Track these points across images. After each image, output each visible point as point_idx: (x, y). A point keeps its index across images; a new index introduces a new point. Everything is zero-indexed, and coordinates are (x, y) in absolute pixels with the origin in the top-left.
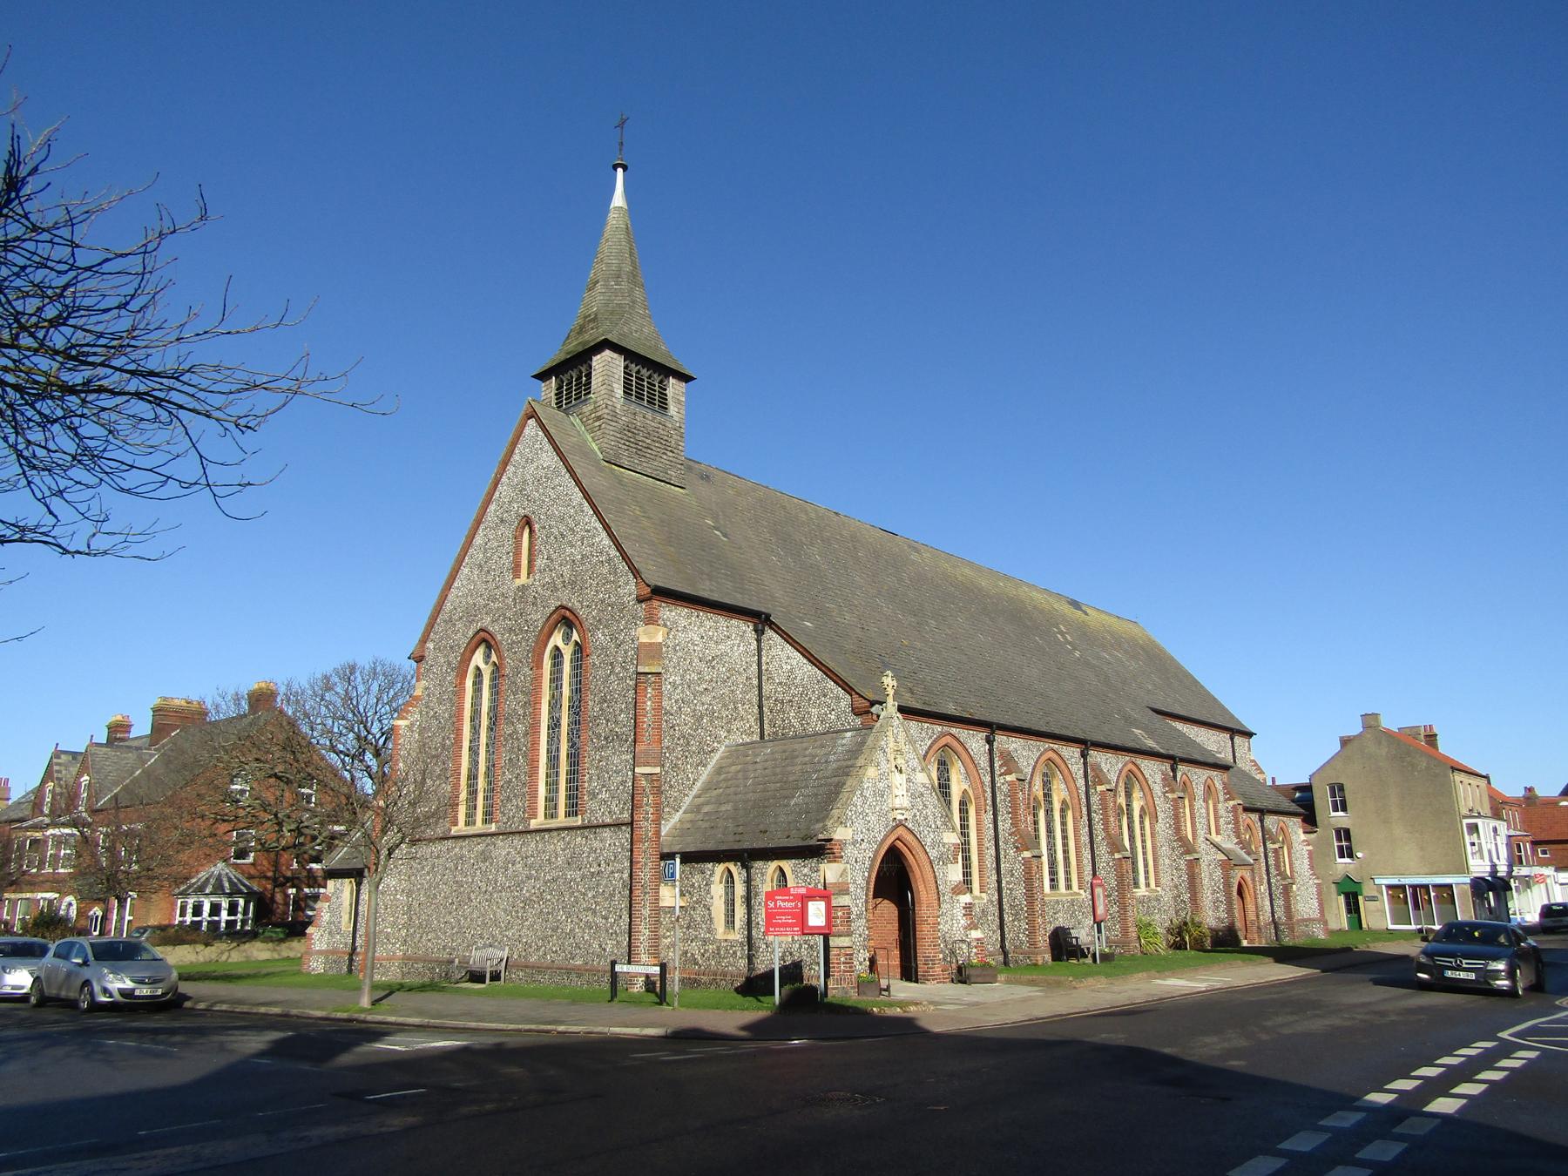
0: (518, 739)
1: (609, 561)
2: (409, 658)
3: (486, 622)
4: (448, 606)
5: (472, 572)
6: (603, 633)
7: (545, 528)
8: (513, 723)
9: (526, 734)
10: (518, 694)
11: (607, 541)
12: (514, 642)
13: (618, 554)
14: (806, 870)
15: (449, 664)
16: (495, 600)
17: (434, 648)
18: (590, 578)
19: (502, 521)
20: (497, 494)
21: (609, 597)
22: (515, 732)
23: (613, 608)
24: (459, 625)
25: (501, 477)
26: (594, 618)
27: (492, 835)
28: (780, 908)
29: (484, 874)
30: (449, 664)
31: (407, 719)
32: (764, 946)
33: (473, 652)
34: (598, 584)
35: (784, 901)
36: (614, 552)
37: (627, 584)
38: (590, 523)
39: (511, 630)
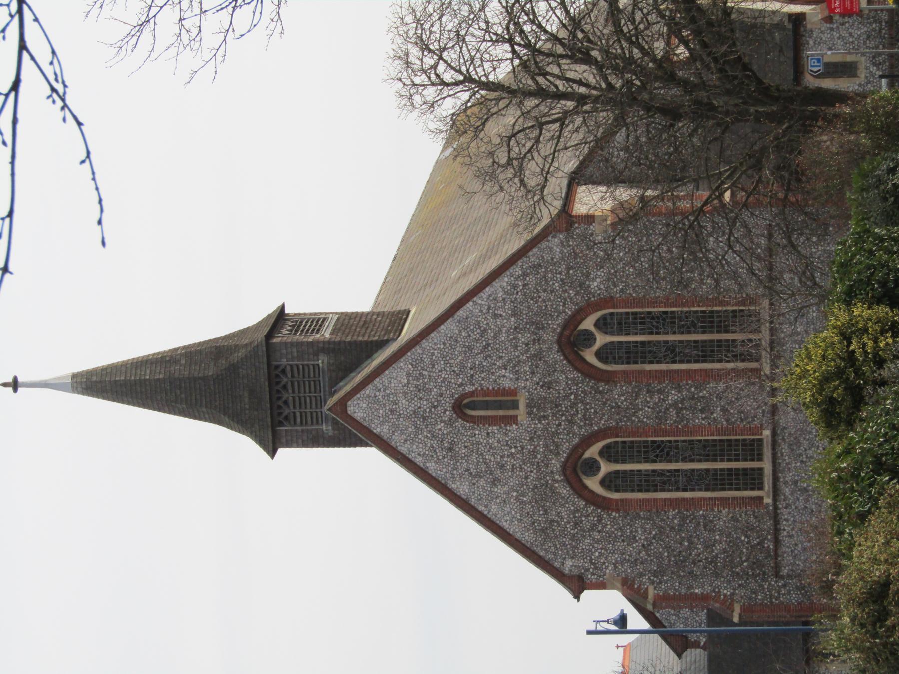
0: (682, 401)
1: (525, 274)
2: (577, 597)
3: (556, 464)
4: (527, 537)
5: (497, 497)
6: (594, 280)
7: (472, 376)
8: (667, 409)
9: (679, 389)
10: (638, 404)
11: (504, 281)
12: (584, 416)
13: (520, 263)
14: (811, 42)
15: (593, 527)
16: (534, 452)
17: (573, 558)
18: (537, 302)
19: (450, 449)
20: (419, 461)
21: (560, 273)
22: (675, 405)
23: (572, 268)
24: (553, 515)
25: (401, 454)
26: (577, 293)
27: (774, 434)
28: (840, 5)
29: (811, 446)
30: (593, 527)
31: (647, 589)
32: (869, 86)
33: (586, 487)
34: (545, 290)
35: (835, 3)
36: (517, 270)
37: (551, 248)
38: (481, 305)
39: (571, 422)
